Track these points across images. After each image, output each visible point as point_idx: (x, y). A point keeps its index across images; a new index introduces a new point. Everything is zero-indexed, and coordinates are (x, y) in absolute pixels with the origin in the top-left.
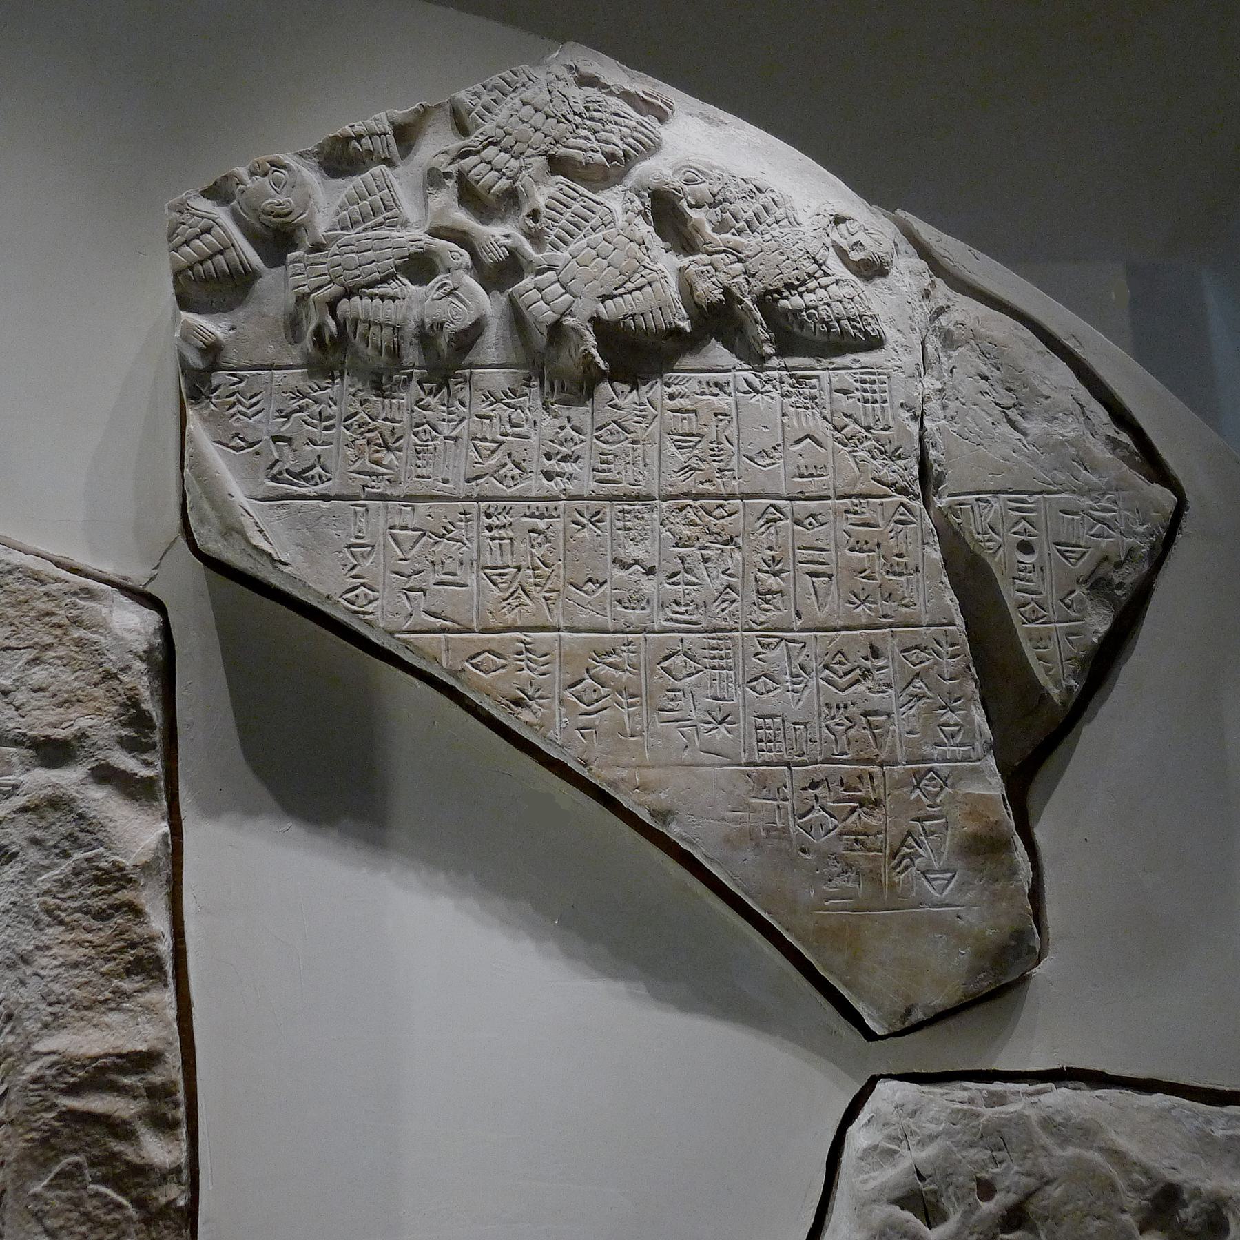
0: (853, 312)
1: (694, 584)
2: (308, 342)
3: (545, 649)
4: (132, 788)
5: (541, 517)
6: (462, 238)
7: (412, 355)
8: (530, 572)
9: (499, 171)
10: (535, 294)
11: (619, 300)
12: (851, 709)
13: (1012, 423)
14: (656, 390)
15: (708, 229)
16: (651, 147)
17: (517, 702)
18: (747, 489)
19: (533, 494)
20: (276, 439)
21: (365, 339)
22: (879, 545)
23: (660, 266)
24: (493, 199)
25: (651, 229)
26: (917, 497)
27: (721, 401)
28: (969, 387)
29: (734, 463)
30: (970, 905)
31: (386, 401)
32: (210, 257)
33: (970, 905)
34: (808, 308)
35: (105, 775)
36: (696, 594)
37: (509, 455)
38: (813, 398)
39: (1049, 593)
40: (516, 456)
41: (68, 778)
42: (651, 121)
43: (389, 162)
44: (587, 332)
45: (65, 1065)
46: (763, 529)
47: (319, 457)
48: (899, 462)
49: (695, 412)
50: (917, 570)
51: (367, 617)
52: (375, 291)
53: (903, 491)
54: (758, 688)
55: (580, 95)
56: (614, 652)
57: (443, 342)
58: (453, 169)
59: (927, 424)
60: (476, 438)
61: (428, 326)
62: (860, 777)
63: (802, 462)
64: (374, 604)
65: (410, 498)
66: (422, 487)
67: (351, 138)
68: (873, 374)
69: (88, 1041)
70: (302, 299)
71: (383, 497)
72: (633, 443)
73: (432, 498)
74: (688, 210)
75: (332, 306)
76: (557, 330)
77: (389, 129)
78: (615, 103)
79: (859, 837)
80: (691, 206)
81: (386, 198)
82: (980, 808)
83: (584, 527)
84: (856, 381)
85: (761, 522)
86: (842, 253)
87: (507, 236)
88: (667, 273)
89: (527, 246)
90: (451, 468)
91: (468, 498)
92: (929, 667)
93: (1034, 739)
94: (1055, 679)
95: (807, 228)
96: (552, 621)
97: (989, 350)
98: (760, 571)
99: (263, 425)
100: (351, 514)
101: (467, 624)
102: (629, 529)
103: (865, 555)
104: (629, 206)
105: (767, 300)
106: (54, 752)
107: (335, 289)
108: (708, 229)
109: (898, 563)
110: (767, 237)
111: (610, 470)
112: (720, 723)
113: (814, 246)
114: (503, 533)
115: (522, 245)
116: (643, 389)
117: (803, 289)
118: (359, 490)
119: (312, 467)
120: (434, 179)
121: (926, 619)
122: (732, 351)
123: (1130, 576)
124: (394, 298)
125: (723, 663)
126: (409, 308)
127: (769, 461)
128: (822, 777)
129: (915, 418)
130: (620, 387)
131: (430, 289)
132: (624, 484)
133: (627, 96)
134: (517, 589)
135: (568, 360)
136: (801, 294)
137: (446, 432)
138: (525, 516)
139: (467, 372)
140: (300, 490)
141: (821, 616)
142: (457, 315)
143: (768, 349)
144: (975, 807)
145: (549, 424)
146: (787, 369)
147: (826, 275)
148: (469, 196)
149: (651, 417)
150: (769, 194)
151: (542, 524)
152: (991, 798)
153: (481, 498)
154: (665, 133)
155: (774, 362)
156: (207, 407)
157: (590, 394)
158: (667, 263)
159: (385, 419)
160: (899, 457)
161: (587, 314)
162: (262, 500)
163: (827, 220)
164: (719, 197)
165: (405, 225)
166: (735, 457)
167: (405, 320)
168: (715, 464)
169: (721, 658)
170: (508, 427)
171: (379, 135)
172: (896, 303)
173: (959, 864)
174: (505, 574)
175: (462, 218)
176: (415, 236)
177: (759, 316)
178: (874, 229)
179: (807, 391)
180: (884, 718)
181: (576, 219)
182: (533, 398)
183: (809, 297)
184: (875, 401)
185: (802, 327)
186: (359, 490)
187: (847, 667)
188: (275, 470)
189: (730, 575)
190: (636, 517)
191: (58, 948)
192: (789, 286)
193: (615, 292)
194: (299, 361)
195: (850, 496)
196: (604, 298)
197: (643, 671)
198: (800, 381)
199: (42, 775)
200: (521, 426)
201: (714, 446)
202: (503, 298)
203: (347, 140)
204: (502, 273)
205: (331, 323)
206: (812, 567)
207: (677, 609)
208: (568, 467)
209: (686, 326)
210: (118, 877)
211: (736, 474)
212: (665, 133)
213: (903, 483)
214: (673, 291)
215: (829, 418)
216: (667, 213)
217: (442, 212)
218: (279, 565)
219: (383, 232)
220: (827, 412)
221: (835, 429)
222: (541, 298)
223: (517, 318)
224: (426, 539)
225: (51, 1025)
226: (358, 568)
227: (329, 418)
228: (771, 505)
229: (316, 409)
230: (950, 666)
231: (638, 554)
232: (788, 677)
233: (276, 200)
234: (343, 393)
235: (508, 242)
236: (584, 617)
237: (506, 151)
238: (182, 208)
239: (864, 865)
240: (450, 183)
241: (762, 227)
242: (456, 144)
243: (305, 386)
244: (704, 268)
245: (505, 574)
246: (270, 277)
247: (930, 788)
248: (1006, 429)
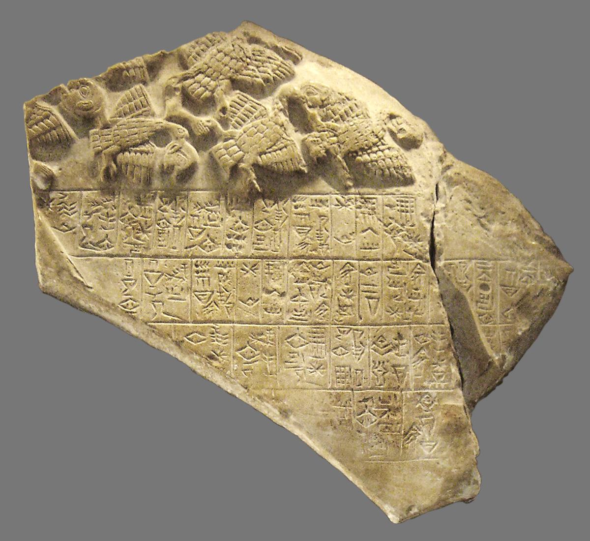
0: (397, 163)
1: (305, 301)
2: (101, 177)
3: (226, 331)
5: (225, 267)
6: (184, 122)
7: (157, 183)
8: (219, 294)
9: (204, 87)
10: (223, 151)
11: (269, 155)
12: (386, 363)
13: (482, 225)
15: (319, 119)
16: (290, 76)
17: (211, 357)
18: (335, 254)
19: (221, 255)
20: (85, 226)
21: (132, 173)
22: (405, 284)
23: (292, 138)
24: (201, 102)
25: (288, 119)
26: (428, 261)
27: (323, 210)
28: (460, 206)
29: (328, 242)
30: (444, 458)
31: (143, 207)
32: (49, 131)
33: (444, 458)
34: (372, 161)
36: (306, 306)
37: (208, 236)
38: (373, 209)
39: (497, 309)
40: (211, 235)
42: (289, 62)
43: (145, 83)
44: (251, 171)
46: (343, 275)
47: (107, 235)
48: (419, 243)
49: (308, 215)
50: (425, 297)
51: (133, 314)
52: (138, 149)
53: (420, 258)
54: (338, 353)
55: (250, 48)
56: (262, 334)
58: (179, 86)
59: (435, 224)
60: (191, 227)
61: (165, 168)
62: (389, 397)
63: (366, 241)
64: (138, 308)
65: (156, 256)
66: (162, 251)
67: (124, 70)
68: (407, 197)
71: (141, 256)
72: (275, 230)
73: (167, 257)
74: (308, 109)
75: (114, 157)
76: (235, 170)
77: (144, 64)
78: (269, 52)
80: (310, 107)
81: (143, 100)
82: (452, 411)
83: (247, 272)
84: (397, 201)
85: (342, 271)
86: (393, 134)
87: (208, 121)
88: (295, 142)
89: (219, 126)
91: (186, 257)
92: (429, 344)
95: (375, 122)
96: (230, 318)
98: (341, 295)
99: (77, 219)
100: (124, 264)
101: (186, 319)
102: (272, 274)
103: (398, 288)
104: (276, 106)
105: (350, 156)
108: (319, 119)
109: (415, 293)
110: (352, 123)
111: (262, 244)
112: (318, 369)
113: (378, 129)
114: (204, 274)
115: (216, 126)
116: (281, 203)
117: (369, 151)
118: (128, 252)
119: (104, 241)
120: (169, 91)
121: (429, 321)
122: (330, 184)
123: (542, 304)
124: (147, 153)
125: (319, 340)
126: (155, 158)
127: (348, 241)
128: (370, 396)
129: (428, 221)
130: (268, 202)
131: (167, 149)
132: (269, 251)
133: (276, 49)
134: (212, 302)
135: (240, 185)
136: (369, 154)
137: (175, 224)
138: (217, 266)
139: (186, 193)
140: (97, 252)
141: (372, 317)
142: (182, 161)
143: (351, 184)
144: (449, 412)
145: (229, 220)
146: (360, 194)
147: (383, 144)
148: (188, 99)
149: (284, 217)
150: (354, 101)
151: (225, 271)
152: (457, 407)
153: (193, 257)
154: (297, 69)
155: (353, 190)
156: (48, 209)
157: (252, 205)
158: (296, 137)
159: (142, 216)
160: (419, 241)
161: (251, 162)
162: (78, 256)
163: (385, 116)
164: (325, 102)
165: (153, 115)
166: (329, 239)
167: (154, 163)
168: (318, 242)
169: (319, 337)
170: (208, 221)
171: (139, 68)
172: (426, 161)
173: (440, 439)
174: (206, 295)
175: (185, 112)
176: (159, 120)
177: (345, 164)
179: (370, 206)
180: (404, 368)
181: (246, 113)
182: (220, 209)
183: (373, 156)
184: (407, 212)
185: (368, 172)
186: (128, 252)
187: (386, 343)
188: (84, 241)
189: (325, 297)
190: (276, 268)
192: (362, 149)
193: (267, 151)
194: (96, 187)
195: (391, 259)
196: (260, 154)
197: (277, 343)
200: (215, 220)
201: (318, 232)
202: (206, 154)
203: (121, 70)
205: (114, 165)
206: (368, 294)
207: (296, 313)
208: (240, 242)
209: (305, 170)
211: (330, 247)
212: (297, 69)
213: (421, 254)
215: (381, 219)
217: (174, 108)
218: (87, 288)
219: (142, 119)
220: (381, 216)
221: (385, 225)
223: (213, 164)
226: (128, 291)
227: (112, 216)
228: (348, 263)
229: (106, 211)
230: (440, 343)
231: (276, 285)
232: (353, 348)
233: (85, 101)
235: (210, 124)
236: (247, 316)
237: (209, 77)
238: (34, 105)
239: (390, 439)
240: (178, 93)
241: (350, 118)
242: (180, 73)
243: (99, 199)
244: (315, 139)
245: (206, 295)
247: (426, 402)
248: (478, 227)
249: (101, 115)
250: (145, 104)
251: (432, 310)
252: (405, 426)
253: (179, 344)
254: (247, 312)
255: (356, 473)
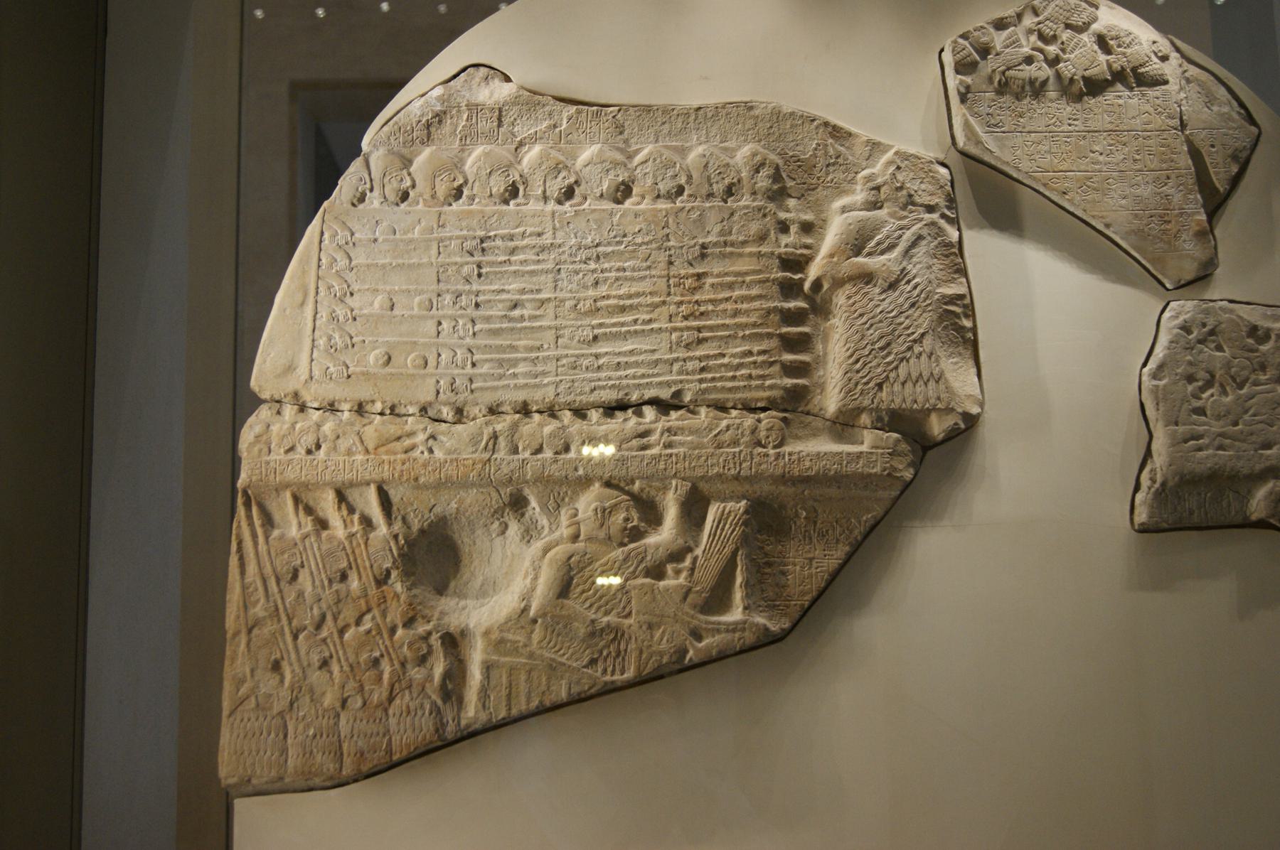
2: (996, 84)
4: (950, 221)
6: (1041, 51)
7: (1027, 88)
14: (1100, 98)
16: (1095, 20)
27: (1121, 102)
28: (1195, 96)
35: (943, 216)
39: (1220, 160)
41: (935, 216)
45: (944, 296)
57: (1037, 84)
66: (1032, 129)
69: (950, 290)
70: (994, 71)
75: (1003, 73)
76: (1072, 80)
79: (1164, 232)
86: (1156, 54)
90: (1040, 124)
93: (1215, 204)
94: (1222, 187)
97: (1201, 84)
105: (1134, 70)
106: (930, 209)
107: (1003, 68)
113: (1148, 52)
123: (1244, 155)
135: (1075, 89)
144: (1199, 223)
145: (1069, 109)
148: (1042, 37)
158: (1102, 58)
172: (1172, 69)
175: (1040, 44)
176: (1026, 50)
178: (1164, 45)
182: (1064, 101)
191: (937, 265)
198: (1144, 95)
199: (927, 216)
204: (1054, 62)
210: (950, 245)
214: (1105, 67)
216: (1102, 41)
222: (1066, 69)
223: (1058, 76)
224: (1035, 144)
225: (939, 286)
230: (1191, 181)
231: (1097, 148)
234: (1007, 100)
236: (1083, 168)
242: (1036, 20)
246: (982, 63)
249: (994, 47)
250: (1018, 40)
251: (1185, 161)
252: (1174, 231)
253: (1045, 185)
254: (1083, 164)
255: (1149, 261)
